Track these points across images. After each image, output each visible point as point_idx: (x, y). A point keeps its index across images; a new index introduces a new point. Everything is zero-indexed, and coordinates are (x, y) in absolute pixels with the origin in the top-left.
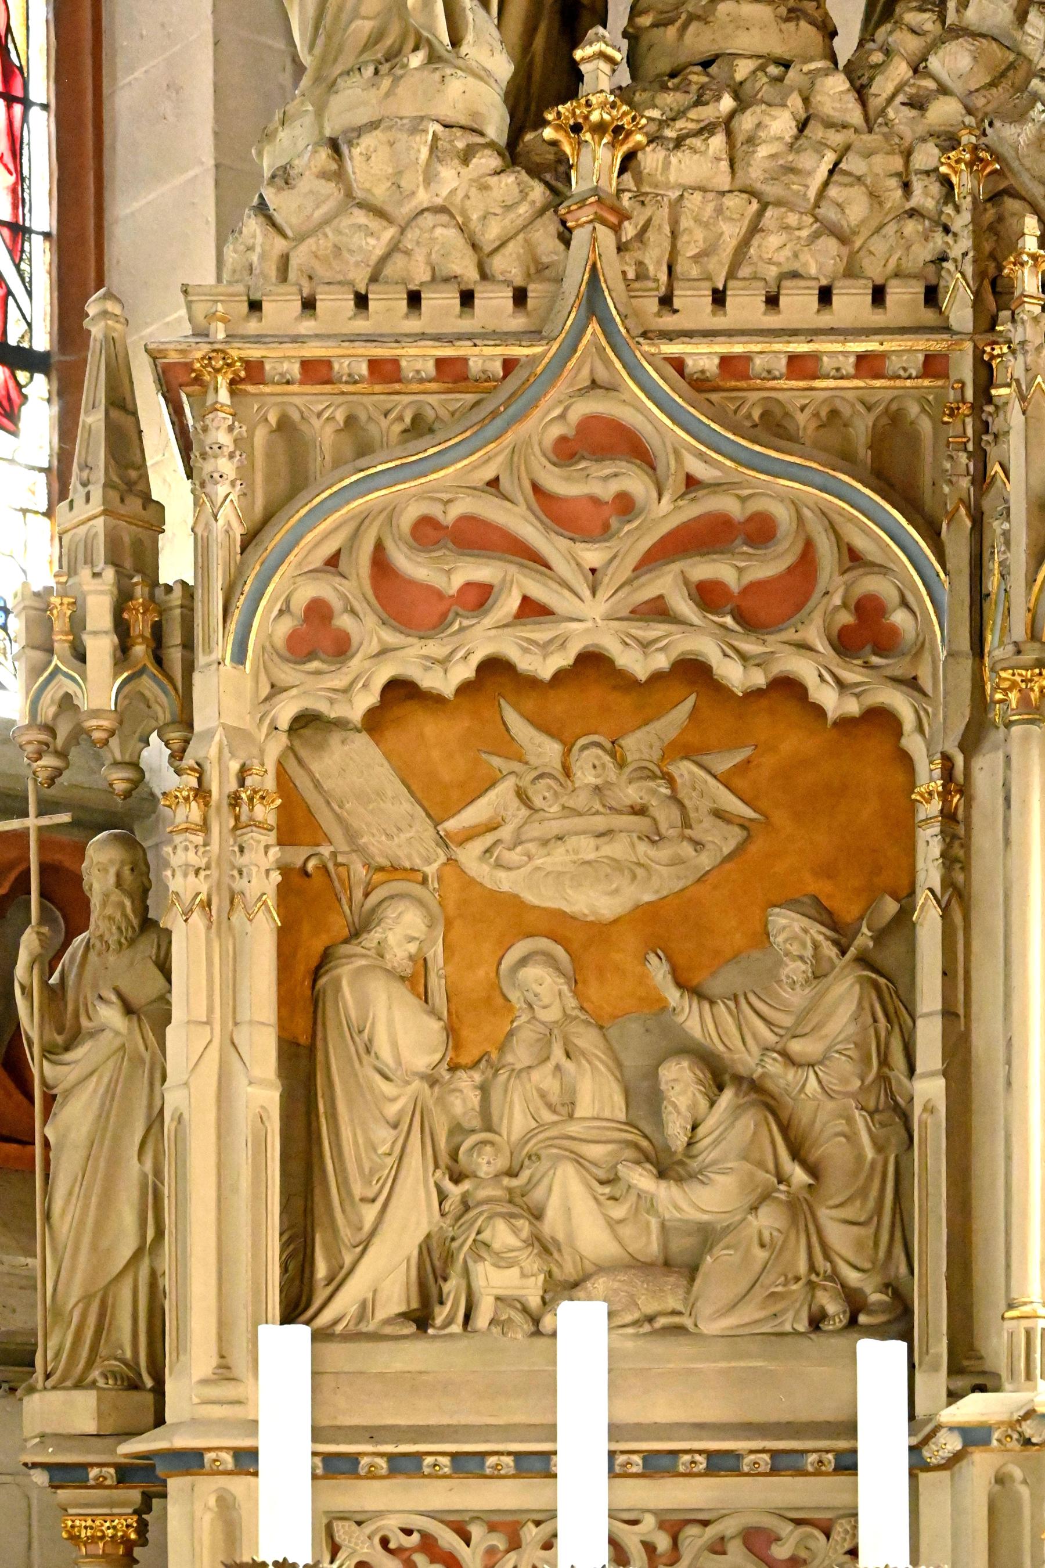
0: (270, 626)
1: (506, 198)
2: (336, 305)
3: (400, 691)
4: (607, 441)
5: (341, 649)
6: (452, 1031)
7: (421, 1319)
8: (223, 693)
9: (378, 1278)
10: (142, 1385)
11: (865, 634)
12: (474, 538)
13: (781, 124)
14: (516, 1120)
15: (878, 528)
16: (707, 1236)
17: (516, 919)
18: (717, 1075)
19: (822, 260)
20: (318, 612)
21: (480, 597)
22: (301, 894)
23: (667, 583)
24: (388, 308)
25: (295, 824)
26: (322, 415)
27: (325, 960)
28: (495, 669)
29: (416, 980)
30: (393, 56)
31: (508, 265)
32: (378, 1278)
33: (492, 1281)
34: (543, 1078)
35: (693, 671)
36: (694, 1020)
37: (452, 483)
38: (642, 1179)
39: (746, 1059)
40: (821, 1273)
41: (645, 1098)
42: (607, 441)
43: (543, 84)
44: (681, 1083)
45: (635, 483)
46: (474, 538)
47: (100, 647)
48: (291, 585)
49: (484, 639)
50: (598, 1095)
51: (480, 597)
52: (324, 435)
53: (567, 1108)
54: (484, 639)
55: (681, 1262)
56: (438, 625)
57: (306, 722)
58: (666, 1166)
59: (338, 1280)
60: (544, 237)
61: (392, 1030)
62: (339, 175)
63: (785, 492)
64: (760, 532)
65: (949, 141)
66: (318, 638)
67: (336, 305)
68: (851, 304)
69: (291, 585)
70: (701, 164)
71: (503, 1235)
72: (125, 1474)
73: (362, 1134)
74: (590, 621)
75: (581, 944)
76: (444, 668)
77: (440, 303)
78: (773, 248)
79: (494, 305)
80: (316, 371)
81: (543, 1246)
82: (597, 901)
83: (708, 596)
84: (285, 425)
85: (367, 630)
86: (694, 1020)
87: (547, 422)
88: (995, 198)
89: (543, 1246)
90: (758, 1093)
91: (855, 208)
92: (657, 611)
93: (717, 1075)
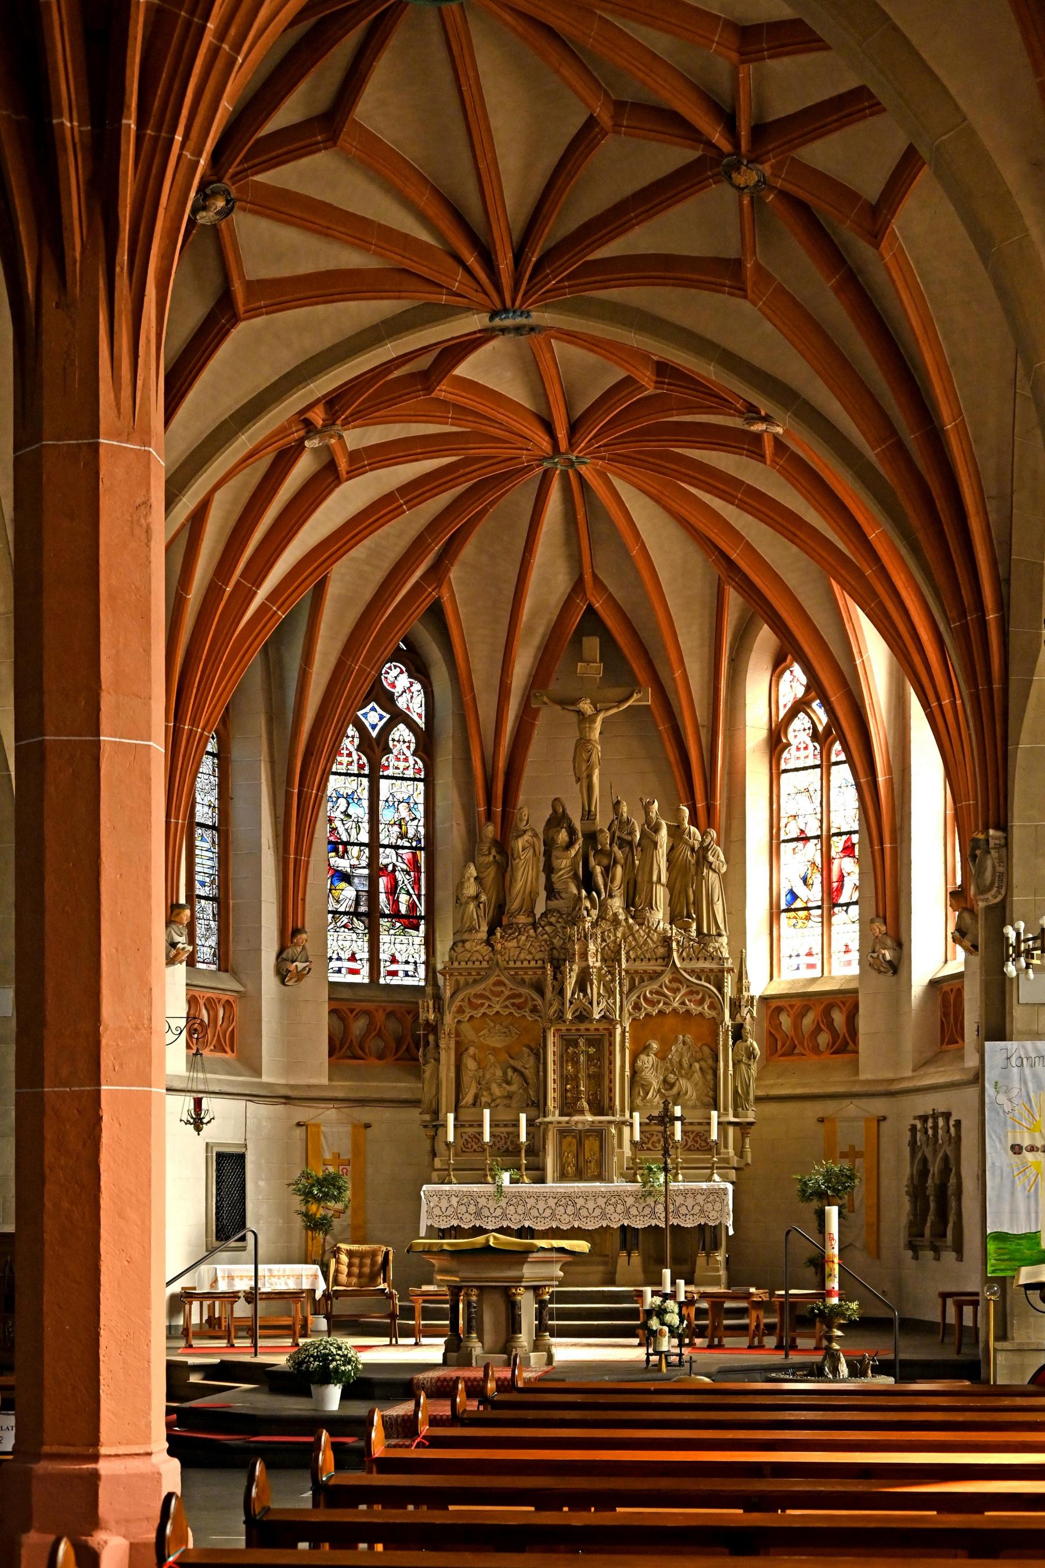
0: (454, 1009)
1: (485, 950)
2: (463, 964)
3: (471, 1017)
4: (500, 983)
5: (464, 1012)
6: (479, 1064)
7: (474, 1104)
8: (449, 1019)
9: (469, 1099)
10: (436, 1113)
11: (534, 1010)
12: (481, 996)
13: (524, 938)
14: (488, 1076)
15: (535, 996)
16: (513, 1093)
17: (489, 1048)
18: (515, 1070)
19: (529, 957)
20: (461, 1006)
21: (482, 1005)
22: (458, 1044)
23: (507, 1003)
24: (470, 965)
25: (458, 1034)
26: (462, 979)
27: (462, 1054)
28: (484, 1014)
29: (474, 1057)
30: (470, 931)
31: (487, 958)
32: (469, 1099)
33: (484, 1099)
34: (492, 1071)
35: (511, 1013)
36: (512, 1062)
37: (479, 989)
38: (504, 1085)
39: (519, 1067)
40: (529, 1097)
41: (505, 1073)
42: (500, 983)
43: (491, 932)
44: (510, 1072)
45: (503, 989)
46: (481, 996)
47: (431, 1010)
48: (457, 1003)
49: (482, 1010)
50: (499, 1073)
51: (482, 1005)
52: (462, 979)
53: (494, 1074)
54: (482, 1010)
55: (510, 1096)
56: (476, 1009)
57: (459, 1022)
58: (508, 1083)
59: (463, 1098)
60: (491, 955)
61: (470, 1064)
62: (463, 946)
63: (523, 991)
64: (520, 996)
65: (546, 941)
66: (461, 1010)
67: (463, 964)
68: (533, 963)
69: (457, 1003)
70: (514, 943)
71: (485, 1093)
72: (434, 1126)
73: (466, 1079)
74: (497, 1008)
75: (494, 1051)
76: (478, 1014)
77: (477, 963)
78: (522, 956)
79: (485, 964)
80: (460, 974)
81: (491, 1094)
82: (499, 1045)
83: (513, 1004)
84: (457, 980)
85: (467, 1010)
86: (512, 1062)
87: (493, 979)
88: (551, 950)
89: (491, 1094)
90: (522, 1074)
91: (533, 950)
92: (506, 1007)
93: (515, 1070)
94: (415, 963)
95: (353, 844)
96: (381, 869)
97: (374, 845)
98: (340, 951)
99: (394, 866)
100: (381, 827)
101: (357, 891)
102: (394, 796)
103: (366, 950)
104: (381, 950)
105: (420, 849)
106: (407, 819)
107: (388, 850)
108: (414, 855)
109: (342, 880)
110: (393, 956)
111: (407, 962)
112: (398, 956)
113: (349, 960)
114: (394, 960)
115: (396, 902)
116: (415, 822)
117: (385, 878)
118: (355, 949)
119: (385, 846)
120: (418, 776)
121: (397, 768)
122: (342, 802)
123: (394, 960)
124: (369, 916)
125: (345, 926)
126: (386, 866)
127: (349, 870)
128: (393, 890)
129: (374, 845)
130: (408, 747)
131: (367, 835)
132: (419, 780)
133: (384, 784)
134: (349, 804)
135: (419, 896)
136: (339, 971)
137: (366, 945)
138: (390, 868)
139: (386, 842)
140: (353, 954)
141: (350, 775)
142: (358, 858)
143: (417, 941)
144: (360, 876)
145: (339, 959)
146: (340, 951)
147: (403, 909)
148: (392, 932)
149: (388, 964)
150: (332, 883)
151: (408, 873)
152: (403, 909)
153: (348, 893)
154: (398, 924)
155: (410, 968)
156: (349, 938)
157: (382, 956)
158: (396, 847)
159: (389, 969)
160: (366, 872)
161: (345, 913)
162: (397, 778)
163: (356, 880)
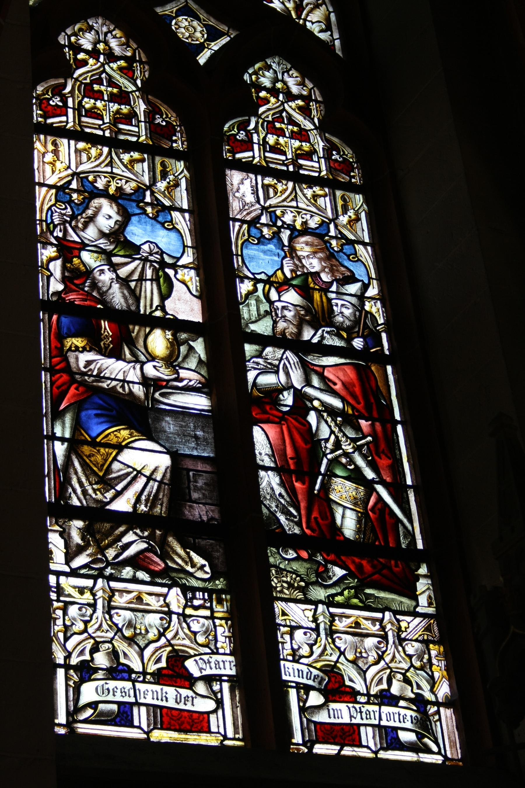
94: (419, 702)
95: (152, 322)
96: (258, 402)
97: (222, 327)
98: (121, 646)
99: (299, 395)
100: (244, 287)
101: (175, 456)
102: (274, 217)
103: (224, 644)
104: (286, 651)
105: (382, 360)
106: (325, 277)
107: (271, 352)
108: (362, 373)
109: (115, 421)
110: (332, 672)
111: (386, 698)
112: (349, 671)
113: (160, 678)
114: (336, 689)
115: (323, 503)
116: (354, 288)
117: (272, 430)
118: (183, 642)
119: (262, 341)
120: (343, 178)
121: (276, 149)
122: (107, 215)
123: (336, 689)
124: (224, 533)
125: (135, 562)
126: (273, 393)
127: (138, 390)
128: (303, 462)
129: (222, 327)
130: (305, 111)
131: (197, 305)
132: (350, 187)
133: (242, 188)
134: (126, 218)
135: (398, 491)
136: (123, 715)
137: (223, 631)
138: (288, 399)
139: (263, 327)
140: (177, 658)
141: (128, 147)
142: (171, 361)
143: (413, 626)
144: (182, 414)
145: (118, 671)
146: (121, 646)
147: (348, 524)
148: (319, 593)
149: (315, 699)
150: (78, 426)
151: (349, 420)
152: (348, 524)
153: (147, 458)
154: (339, 572)
155: (401, 718)
156: (154, 603)
157: (290, 672)
158: (300, 348)
159: (322, 717)
160: (200, 402)
161: (131, 520)
162: (280, 176)
163: (170, 426)
